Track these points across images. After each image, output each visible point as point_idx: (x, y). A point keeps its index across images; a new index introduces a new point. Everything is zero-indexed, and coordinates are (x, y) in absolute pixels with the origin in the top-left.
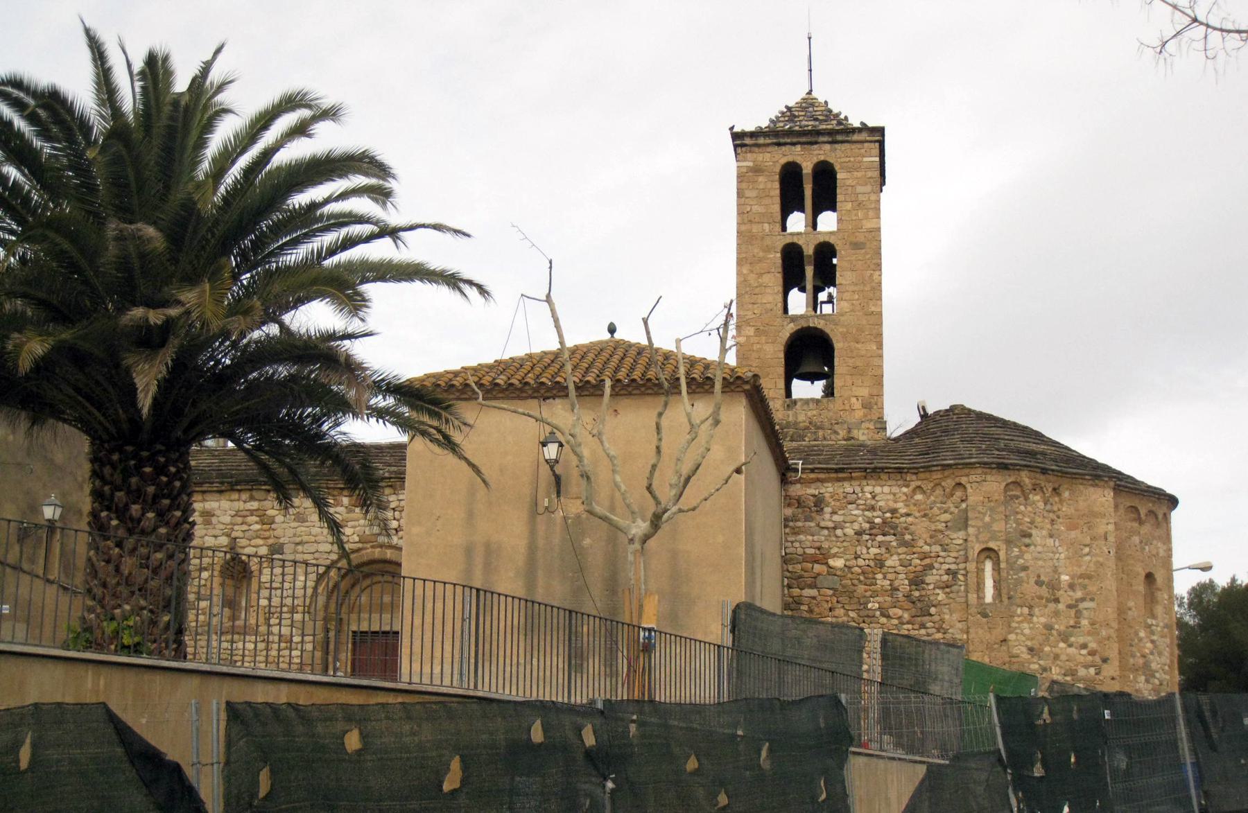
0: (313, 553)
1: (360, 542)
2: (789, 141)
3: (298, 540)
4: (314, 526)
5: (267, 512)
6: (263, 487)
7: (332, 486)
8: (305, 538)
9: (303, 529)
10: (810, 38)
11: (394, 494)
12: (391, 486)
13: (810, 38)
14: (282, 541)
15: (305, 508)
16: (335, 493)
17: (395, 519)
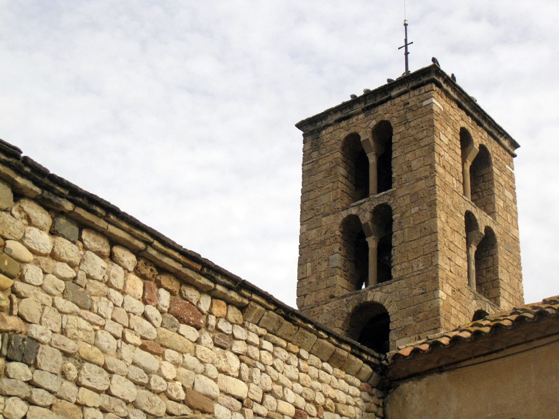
0: (99, 392)
1: (184, 402)
2: (467, 108)
3: (71, 346)
4: (103, 327)
5: (9, 244)
6: (20, 180)
7: (154, 252)
8: (86, 350)
9: (84, 324)
10: (406, 25)
11: (243, 325)
12: (242, 308)
13: (406, 25)
14: (36, 331)
15: (88, 276)
16: (147, 271)
17: (240, 377)
